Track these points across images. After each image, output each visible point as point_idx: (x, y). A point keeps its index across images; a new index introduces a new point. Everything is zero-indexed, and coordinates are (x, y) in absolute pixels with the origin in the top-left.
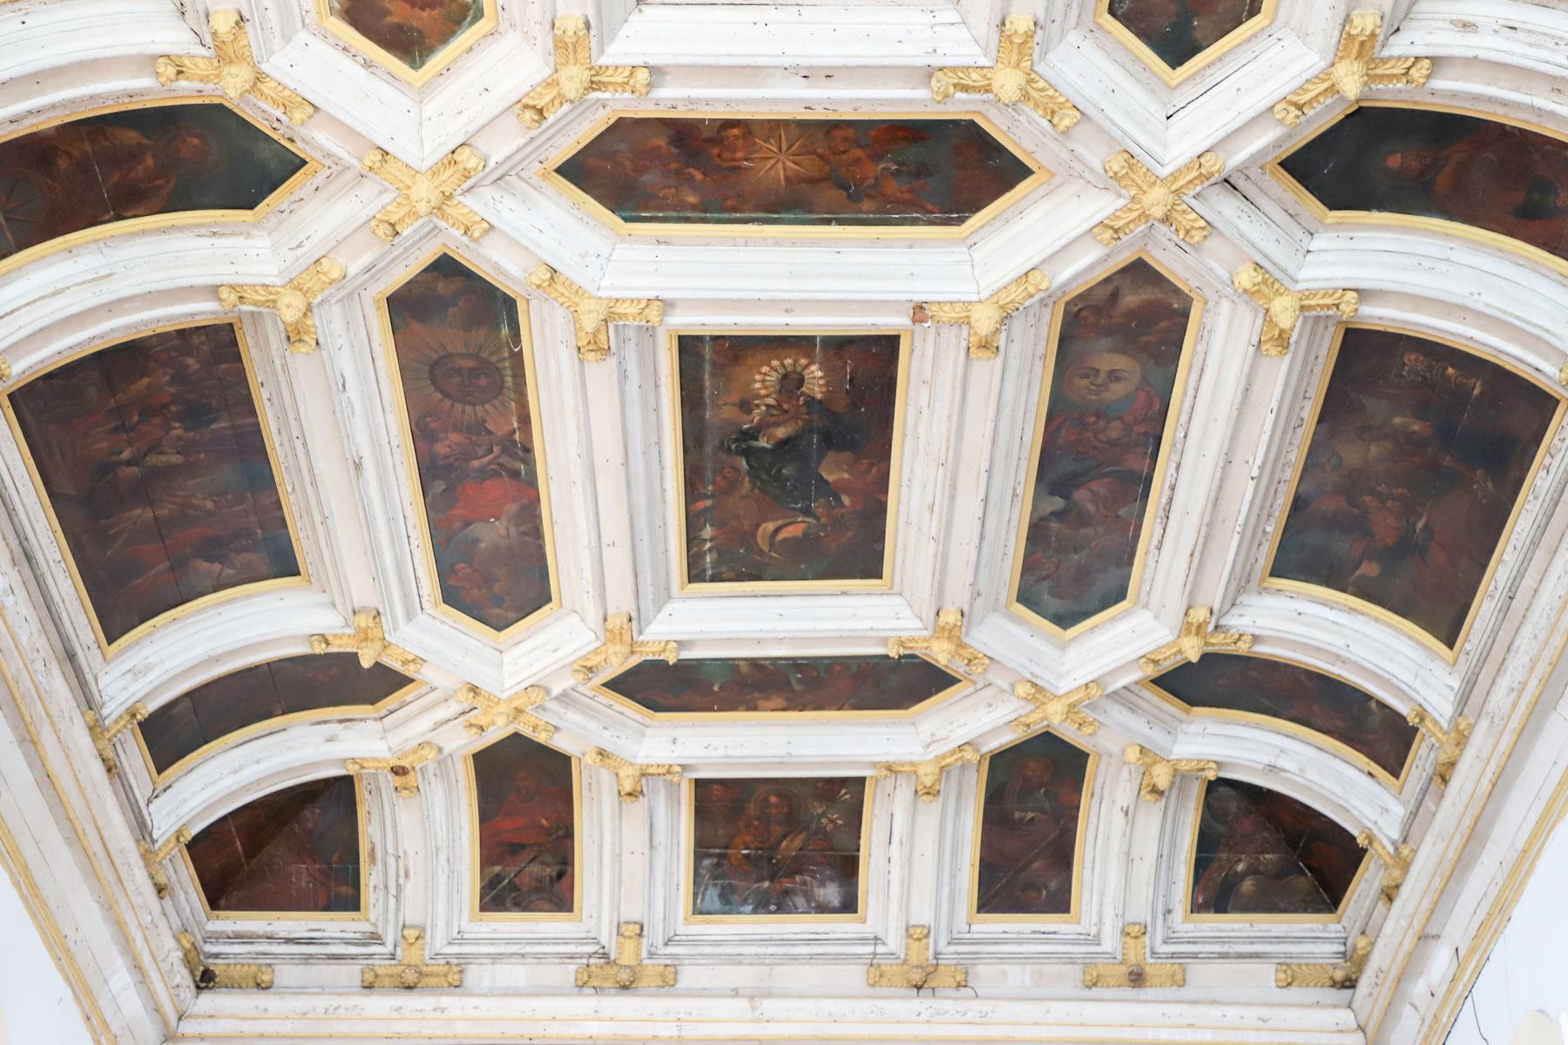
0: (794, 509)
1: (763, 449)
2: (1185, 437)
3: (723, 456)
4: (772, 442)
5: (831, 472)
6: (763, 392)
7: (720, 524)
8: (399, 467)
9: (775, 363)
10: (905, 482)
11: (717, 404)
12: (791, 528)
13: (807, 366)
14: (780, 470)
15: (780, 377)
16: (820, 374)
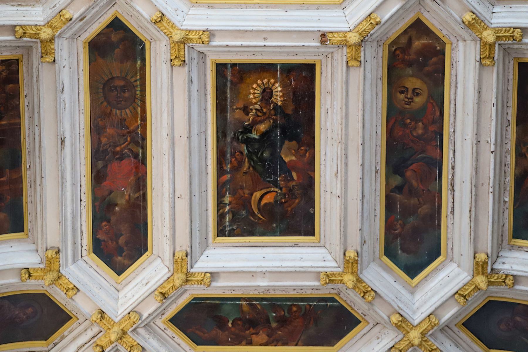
0: (269, 181)
1: (254, 139)
2: (454, 132)
3: (235, 144)
4: (258, 134)
5: (286, 156)
6: (254, 101)
7: (233, 193)
8: (82, 149)
9: (259, 82)
10: (323, 162)
11: (233, 109)
12: (268, 196)
13: (274, 84)
14: (262, 154)
15: (262, 90)
16: (280, 89)
